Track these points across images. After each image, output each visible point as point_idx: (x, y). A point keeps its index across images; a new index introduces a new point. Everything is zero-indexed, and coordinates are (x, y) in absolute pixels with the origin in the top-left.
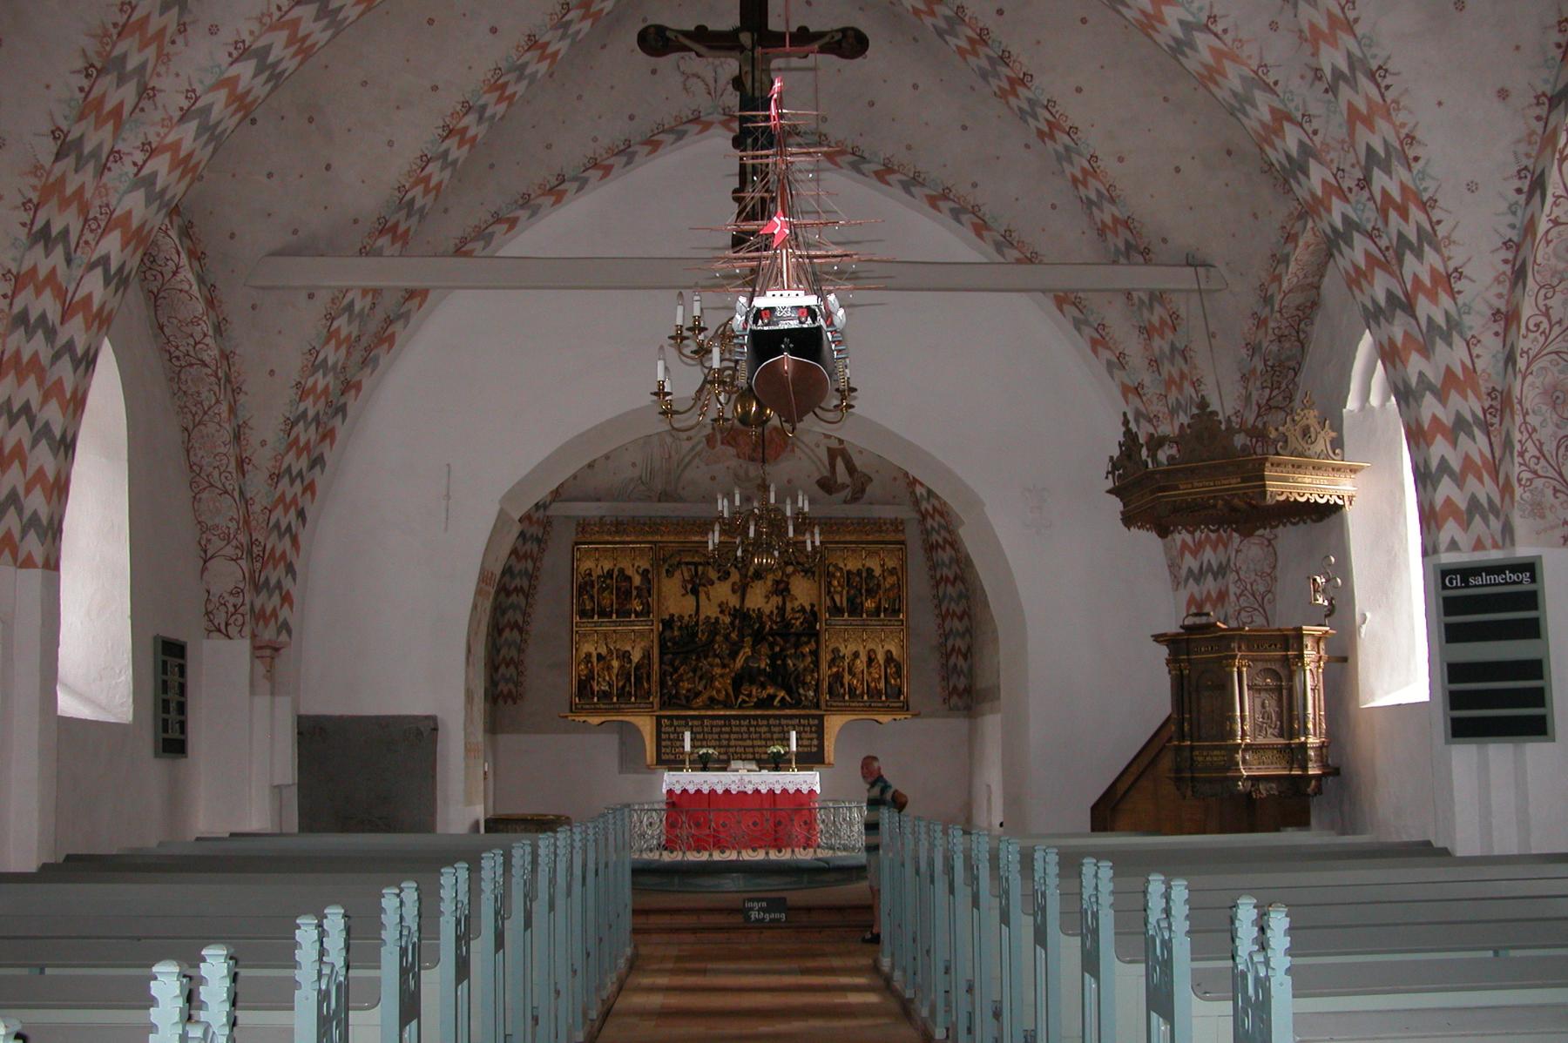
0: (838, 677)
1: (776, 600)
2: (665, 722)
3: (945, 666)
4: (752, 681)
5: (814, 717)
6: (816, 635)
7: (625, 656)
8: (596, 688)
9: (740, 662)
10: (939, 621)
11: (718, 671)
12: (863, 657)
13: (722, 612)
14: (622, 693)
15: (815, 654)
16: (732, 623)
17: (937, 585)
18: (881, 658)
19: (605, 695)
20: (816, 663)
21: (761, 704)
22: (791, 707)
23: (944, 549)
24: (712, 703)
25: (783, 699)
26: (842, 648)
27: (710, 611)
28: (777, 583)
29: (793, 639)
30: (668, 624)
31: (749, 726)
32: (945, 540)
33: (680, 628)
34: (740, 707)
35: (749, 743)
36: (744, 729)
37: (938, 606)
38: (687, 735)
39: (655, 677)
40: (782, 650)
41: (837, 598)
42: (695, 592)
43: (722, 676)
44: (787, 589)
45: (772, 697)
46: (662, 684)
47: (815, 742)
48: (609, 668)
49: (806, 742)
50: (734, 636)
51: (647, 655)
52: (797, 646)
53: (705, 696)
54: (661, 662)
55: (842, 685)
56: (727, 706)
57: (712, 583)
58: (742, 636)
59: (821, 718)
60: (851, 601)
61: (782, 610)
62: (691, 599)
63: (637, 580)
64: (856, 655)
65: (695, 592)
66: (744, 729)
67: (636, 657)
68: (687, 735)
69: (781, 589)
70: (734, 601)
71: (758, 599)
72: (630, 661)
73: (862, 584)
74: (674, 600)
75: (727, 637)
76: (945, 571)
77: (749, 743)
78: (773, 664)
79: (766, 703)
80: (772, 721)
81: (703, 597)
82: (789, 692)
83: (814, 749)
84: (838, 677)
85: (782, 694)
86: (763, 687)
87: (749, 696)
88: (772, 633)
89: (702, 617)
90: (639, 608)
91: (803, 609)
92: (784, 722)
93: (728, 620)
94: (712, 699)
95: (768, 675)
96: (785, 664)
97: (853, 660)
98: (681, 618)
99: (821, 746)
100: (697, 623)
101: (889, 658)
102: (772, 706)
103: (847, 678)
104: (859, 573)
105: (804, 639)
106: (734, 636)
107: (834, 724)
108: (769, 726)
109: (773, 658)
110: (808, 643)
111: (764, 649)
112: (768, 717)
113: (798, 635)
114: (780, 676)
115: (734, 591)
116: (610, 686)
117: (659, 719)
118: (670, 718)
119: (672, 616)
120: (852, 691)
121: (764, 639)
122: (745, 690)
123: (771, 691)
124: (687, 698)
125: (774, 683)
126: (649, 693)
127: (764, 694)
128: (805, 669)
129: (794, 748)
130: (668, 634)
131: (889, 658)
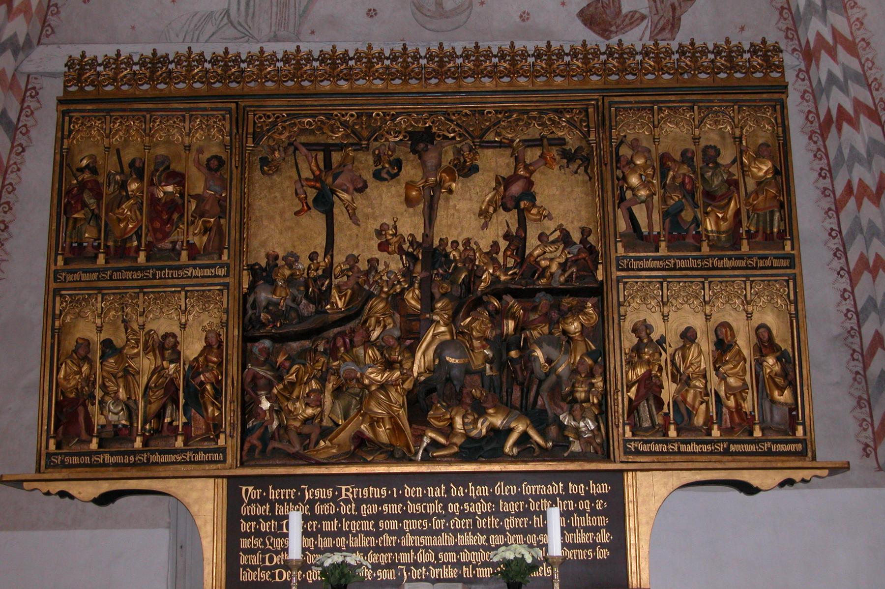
0: (649, 387)
1: (505, 220)
2: (250, 491)
3: (861, 376)
4: (456, 399)
5: (599, 476)
6: (598, 292)
7: (167, 347)
8: (99, 420)
9: (420, 362)
10: (844, 283)
11: (376, 376)
12: (705, 343)
13: (383, 247)
14: (160, 430)
15: (598, 334)
16: (408, 273)
17: (838, 206)
18: (744, 343)
19: (115, 436)
20: (600, 355)
21: (473, 449)
22: (544, 455)
23: (854, 123)
24: (362, 448)
25: (525, 437)
26: (654, 320)
27: (356, 243)
28: (505, 182)
30: (263, 274)
31: (445, 501)
32: (858, 105)
33: (290, 281)
34: (427, 459)
35: (446, 540)
36: (435, 508)
37: (842, 252)
38: (295, 520)
39: (230, 392)
40: (519, 329)
41: (640, 213)
42: (324, 202)
43: (383, 387)
44: (529, 195)
45: (499, 435)
46: (248, 408)
47: (604, 537)
48: (128, 375)
49: (582, 538)
50: (412, 299)
51: (214, 345)
53: (344, 436)
54: (245, 358)
55: (660, 403)
56: (392, 455)
57: (362, 189)
58: (428, 301)
59: (616, 479)
60: (672, 216)
61: (516, 241)
62: (315, 222)
63: (198, 183)
64: (688, 336)
65: (324, 202)
66: (438, 508)
67: (192, 348)
68: (295, 520)
69: (516, 196)
70: (411, 225)
71: (466, 219)
72: (176, 357)
73: (695, 182)
74: (281, 228)
75: (396, 301)
76: (859, 173)
77: (446, 540)
78: (500, 362)
79: (486, 447)
80: (500, 489)
81: (340, 215)
82: (540, 421)
83: (602, 554)
84: (649, 387)
85: (520, 427)
86: (480, 411)
87: (448, 430)
88: (497, 290)
89: (339, 258)
90: (200, 241)
91: (565, 238)
92: (528, 489)
93: (396, 264)
94: (360, 440)
95: (491, 385)
96: (527, 358)
97: (684, 349)
98: (292, 259)
99: (619, 546)
100: (328, 272)
101: (765, 343)
102: (497, 455)
103: (669, 390)
104: (687, 158)
105: (567, 302)
106: (412, 299)
107: (649, 492)
108: (493, 498)
109: (502, 344)
111: (477, 324)
112: (489, 478)
113: (556, 293)
114: (513, 381)
115: (409, 202)
116: (131, 415)
117: (234, 484)
118: (260, 482)
119: (273, 258)
120: (683, 414)
121: (479, 302)
122: (437, 414)
123: (498, 421)
124: (303, 437)
125: (506, 405)
126: (216, 427)
127: (482, 428)
128: (574, 371)
129: (556, 549)
130: (264, 295)
131: (765, 343)
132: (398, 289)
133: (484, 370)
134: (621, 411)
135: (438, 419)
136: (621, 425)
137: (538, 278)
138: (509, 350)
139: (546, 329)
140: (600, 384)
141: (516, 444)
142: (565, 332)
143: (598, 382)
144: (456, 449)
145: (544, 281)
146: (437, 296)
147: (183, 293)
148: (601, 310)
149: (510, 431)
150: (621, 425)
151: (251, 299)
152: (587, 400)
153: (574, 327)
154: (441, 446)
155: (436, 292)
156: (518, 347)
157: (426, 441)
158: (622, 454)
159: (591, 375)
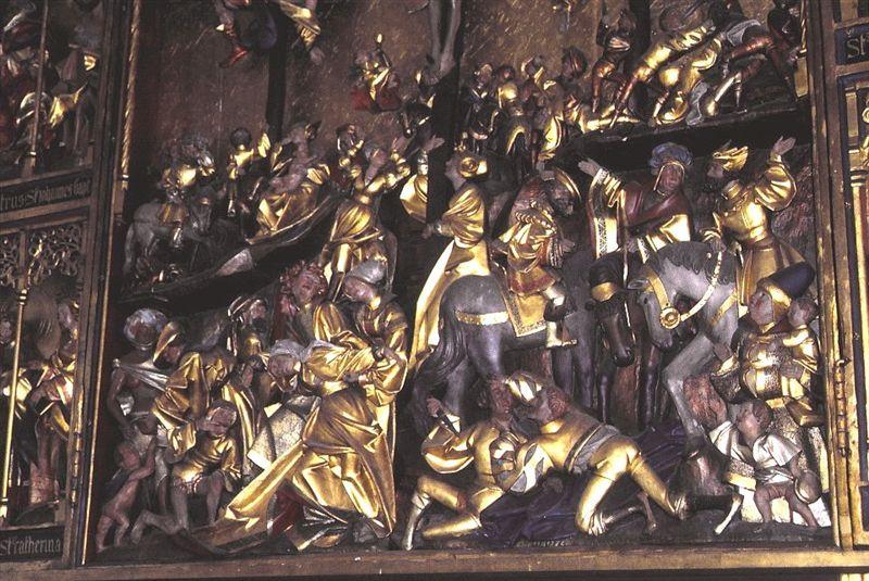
25: (626, 485)
29: (672, 167)
52: (703, 198)
85: (621, 459)
110: (752, 176)
113: (700, 141)
123: (555, 450)
132: (392, 180)
133: (544, 334)
134: (853, 416)
135: (449, 454)
136: (854, 449)
137: (662, 111)
138: (596, 282)
139: (680, 229)
140: (808, 350)
141: (603, 508)
142: (731, 235)
143: (801, 340)
144: (472, 524)
145: (669, 117)
146: (458, 183)
147: (23, 238)
148: (794, 163)
149: (592, 472)
150: (854, 449)
151: (130, 233)
152: (775, 393)
153: (753, 217)
154: (454, 515)
155: (457, 176)
156: (616, 279)
157: (420, 503)
158: (859, 526)
159: (785, 325)
